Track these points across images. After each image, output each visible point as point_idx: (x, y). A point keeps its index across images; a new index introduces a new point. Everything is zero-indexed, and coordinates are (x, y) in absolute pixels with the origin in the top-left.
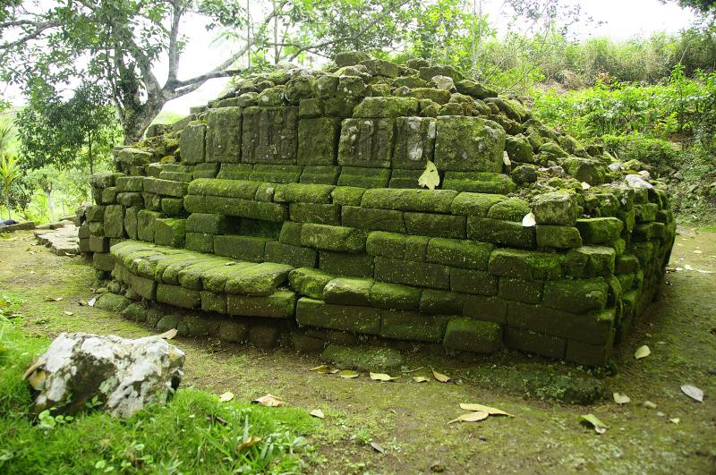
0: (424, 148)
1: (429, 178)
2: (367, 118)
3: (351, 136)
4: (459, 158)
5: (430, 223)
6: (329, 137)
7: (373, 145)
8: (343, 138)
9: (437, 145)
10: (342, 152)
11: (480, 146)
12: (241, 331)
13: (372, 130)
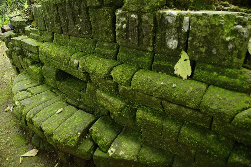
0: (179, 40)
1: (183, 67)
2: (132, 12)
3: (122, 25)
4: (209, 52)
5: (182, 114)
6: (109, 23)
7: (139, 34)
8: (118, 26)
9: (190, 38)
10: (119, 36)
11: (230, 46)
12: (68, 157)
13: (137, 22)
